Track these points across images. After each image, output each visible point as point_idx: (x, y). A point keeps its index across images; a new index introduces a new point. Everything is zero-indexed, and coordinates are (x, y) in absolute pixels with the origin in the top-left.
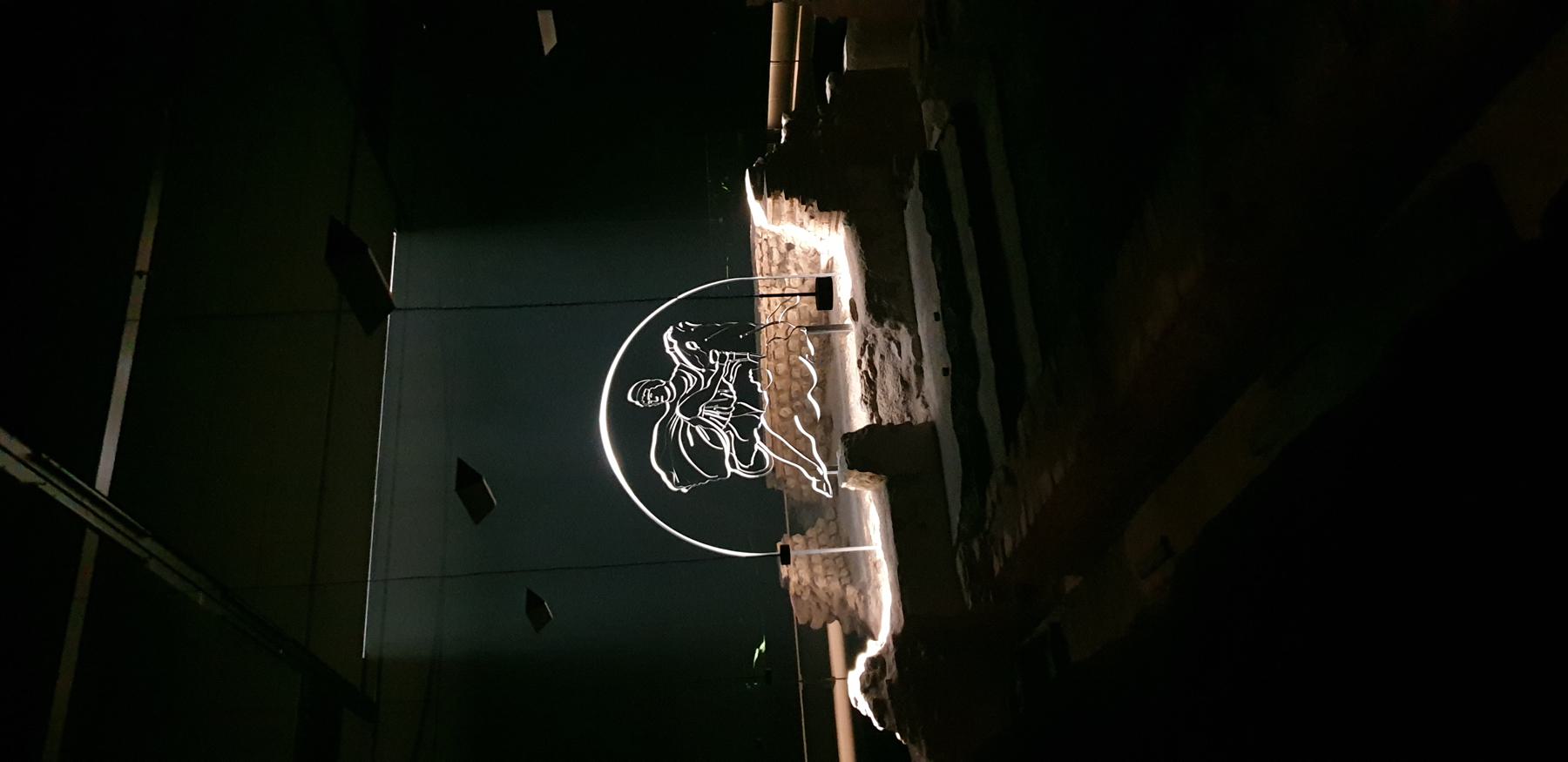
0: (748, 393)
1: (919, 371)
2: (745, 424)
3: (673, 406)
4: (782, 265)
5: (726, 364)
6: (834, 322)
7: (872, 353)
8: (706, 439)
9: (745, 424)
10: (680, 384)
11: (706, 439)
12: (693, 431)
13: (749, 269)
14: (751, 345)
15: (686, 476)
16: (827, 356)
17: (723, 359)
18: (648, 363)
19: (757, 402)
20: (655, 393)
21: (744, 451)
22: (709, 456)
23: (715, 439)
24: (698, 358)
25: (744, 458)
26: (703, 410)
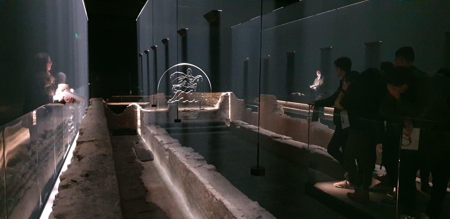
2: (183, 89)
4: (216, 98)
5: (193, 86)
7: (194, 112)
9: (183, 89)
10: (191, 77)
13: (213, 92)
14: (198, 91)
15: (173, 78)
16: (194, 104)
18: (195, 72)
19: (186, 91)
20: (189, 73)
21: (178, 88)
22: (177, 82)
24: (195, 81)
25: (176, 88)
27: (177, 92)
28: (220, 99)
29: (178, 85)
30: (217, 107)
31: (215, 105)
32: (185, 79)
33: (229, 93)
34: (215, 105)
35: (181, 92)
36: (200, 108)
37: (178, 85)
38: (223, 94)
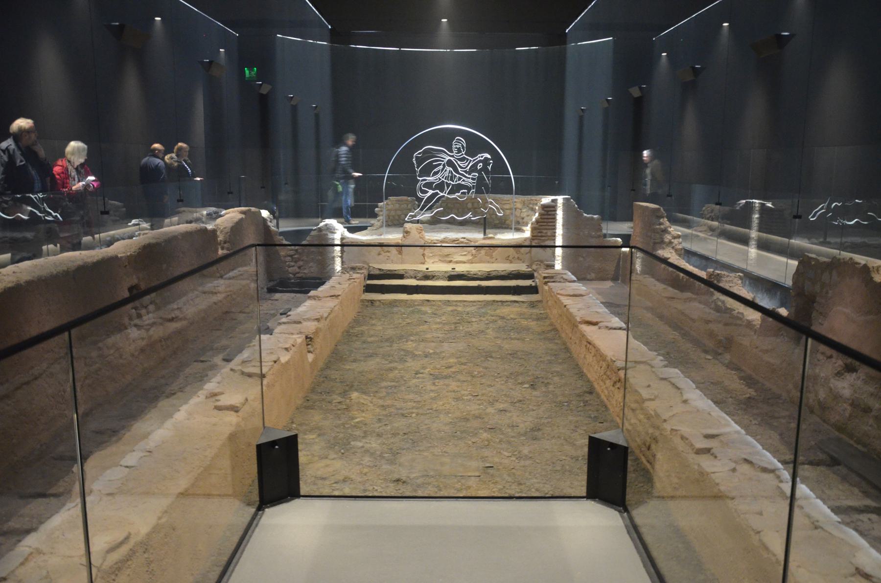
0: (456, 189)
1: (450, 262)
2: (441, 186)
3: (452, 156)
5: (469, 180)
6: (487, 231)
8: (435, 170)
11: (435, 170)
12: (440, 165)
14: (479, 191)
15: (420, 161)
17: (473, 179)
21: (429, 185)
23: (436, 173)
24: (474, 169)
25: (426, 185)
26: (449, 169)
27: (428, 195)
28: (537, 214)
29: (430, 179)
30: (527, 233)
31: (524, 228)
32: (450, 163)
33: (560, 199)
34: (524, 228)
35: (437, 194)
36: (485, 234)
37: (430, 179)
38: (546, 200)
